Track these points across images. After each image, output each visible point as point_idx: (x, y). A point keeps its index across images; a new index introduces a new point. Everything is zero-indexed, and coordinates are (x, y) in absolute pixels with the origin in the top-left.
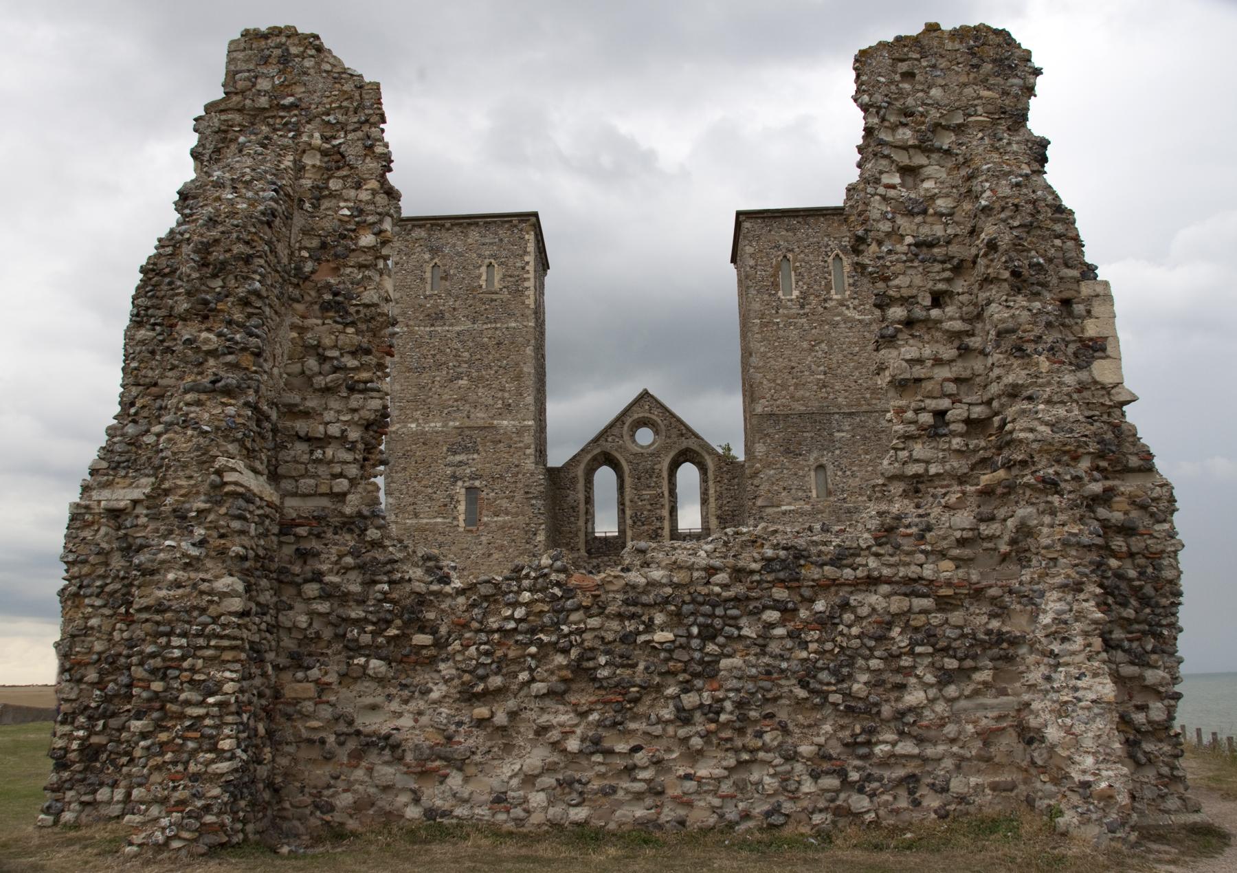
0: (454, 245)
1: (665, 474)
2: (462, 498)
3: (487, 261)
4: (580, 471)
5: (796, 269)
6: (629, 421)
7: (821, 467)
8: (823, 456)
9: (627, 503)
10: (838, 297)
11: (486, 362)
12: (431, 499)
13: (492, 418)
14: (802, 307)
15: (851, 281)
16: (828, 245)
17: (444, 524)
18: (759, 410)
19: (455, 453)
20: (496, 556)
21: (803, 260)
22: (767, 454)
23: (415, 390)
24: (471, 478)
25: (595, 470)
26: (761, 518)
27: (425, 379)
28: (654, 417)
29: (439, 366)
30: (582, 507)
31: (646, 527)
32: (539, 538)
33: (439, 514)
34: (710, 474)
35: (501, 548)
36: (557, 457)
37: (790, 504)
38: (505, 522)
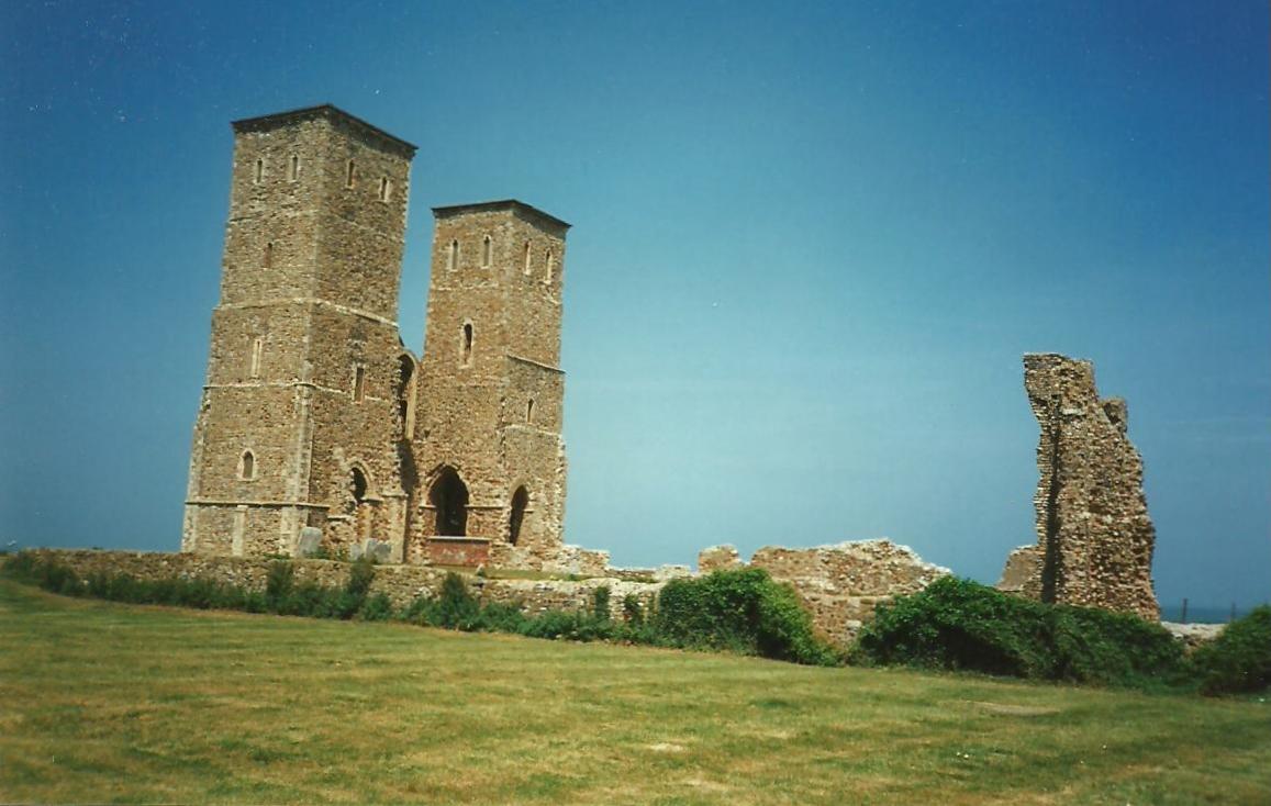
19: (354, 337)
27: (339, 262)
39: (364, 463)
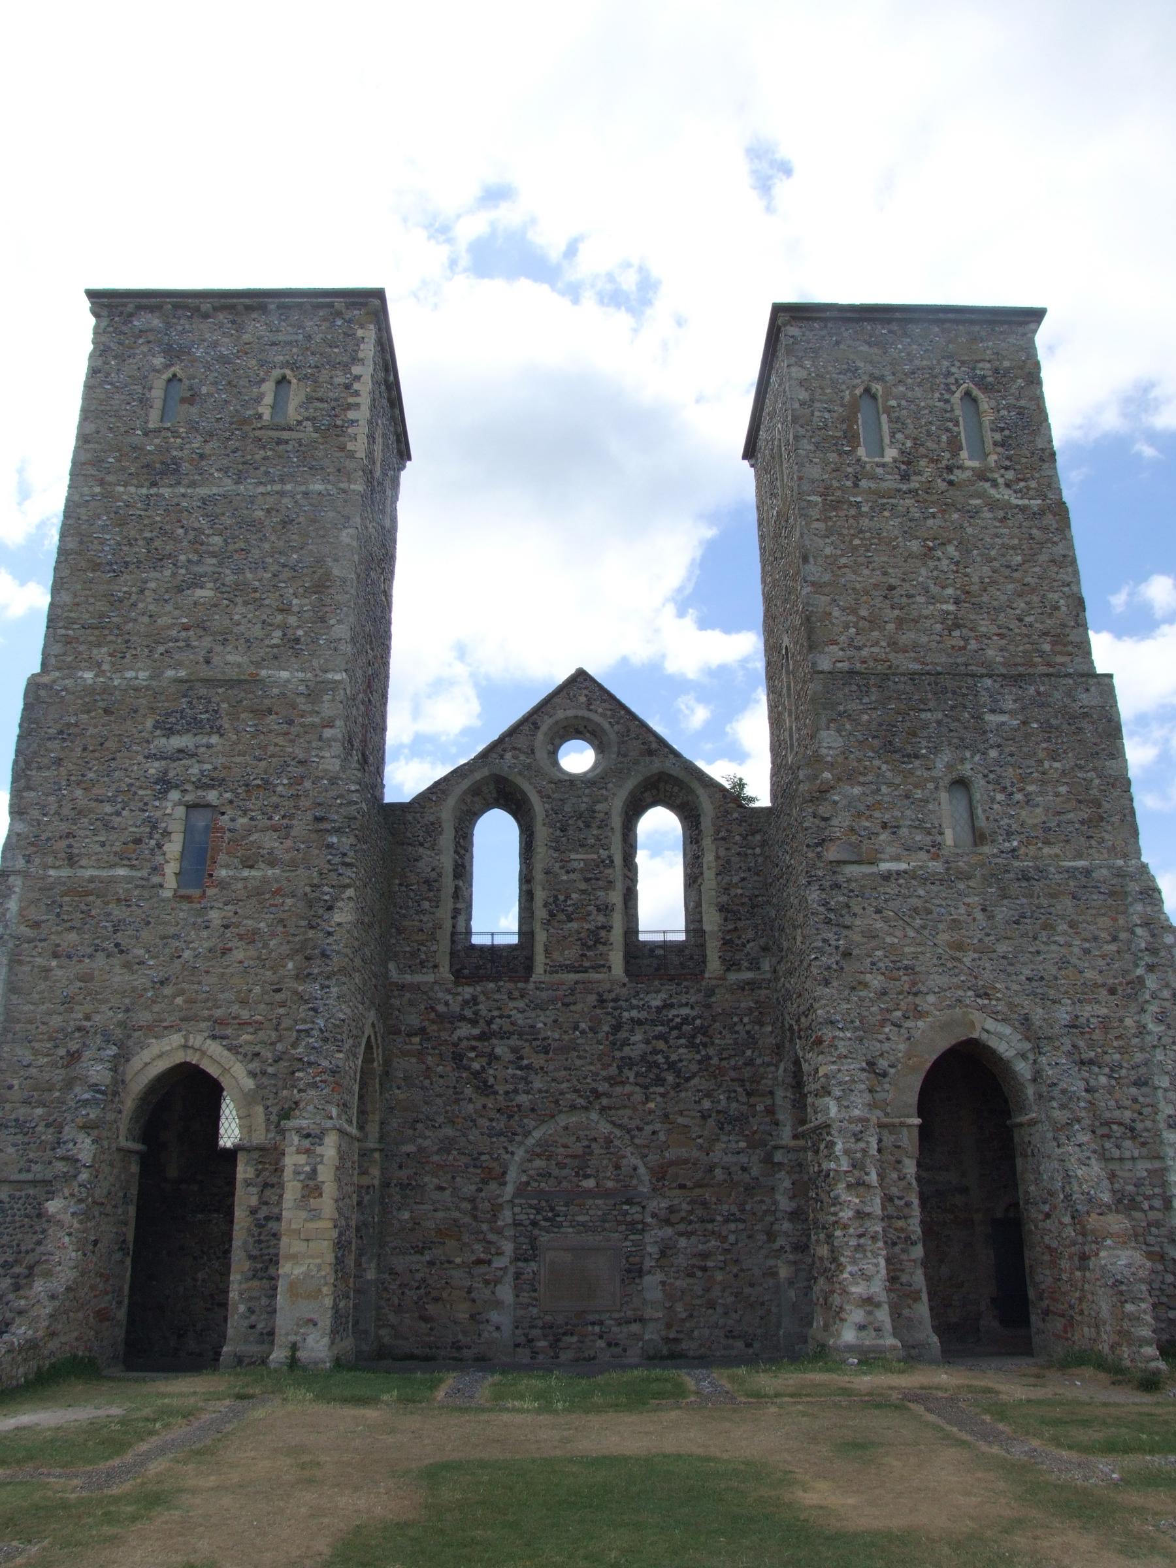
0: (215, 345)
1: (617, 821)
2: (176, 828)
3: (276, 373)
4: (447, 813)
5: (888, 410)
6: (546, 724)
7: (961, 783)
8: (963, 760)
9: (539, 876)
10: (975, 464)
11: (256, 554)
12: (109, 827)
13: (258, 665)
14: (905, 478)
15: (998, 437)
16: (949, 374)
17: (129, 880)
18: (825, 664)
19: (170, 732)
20: (239, 955)
21: (904, 397)
22: (845, 752)
23: (101, 606)
24: (200, 785)
25: (475, 815)
26: (836, 886)
27: (125, 585)
28: (596, 718)
29: (158, 560)
30: (448, 883)
31: (574, 925)
32: (338, 917)
33: (122, 858)
34: (707, 823)
35: (251, 937)
36: (406, 778)
37: (897, 858)
38: (265, 880)
39: (215, 1048)
